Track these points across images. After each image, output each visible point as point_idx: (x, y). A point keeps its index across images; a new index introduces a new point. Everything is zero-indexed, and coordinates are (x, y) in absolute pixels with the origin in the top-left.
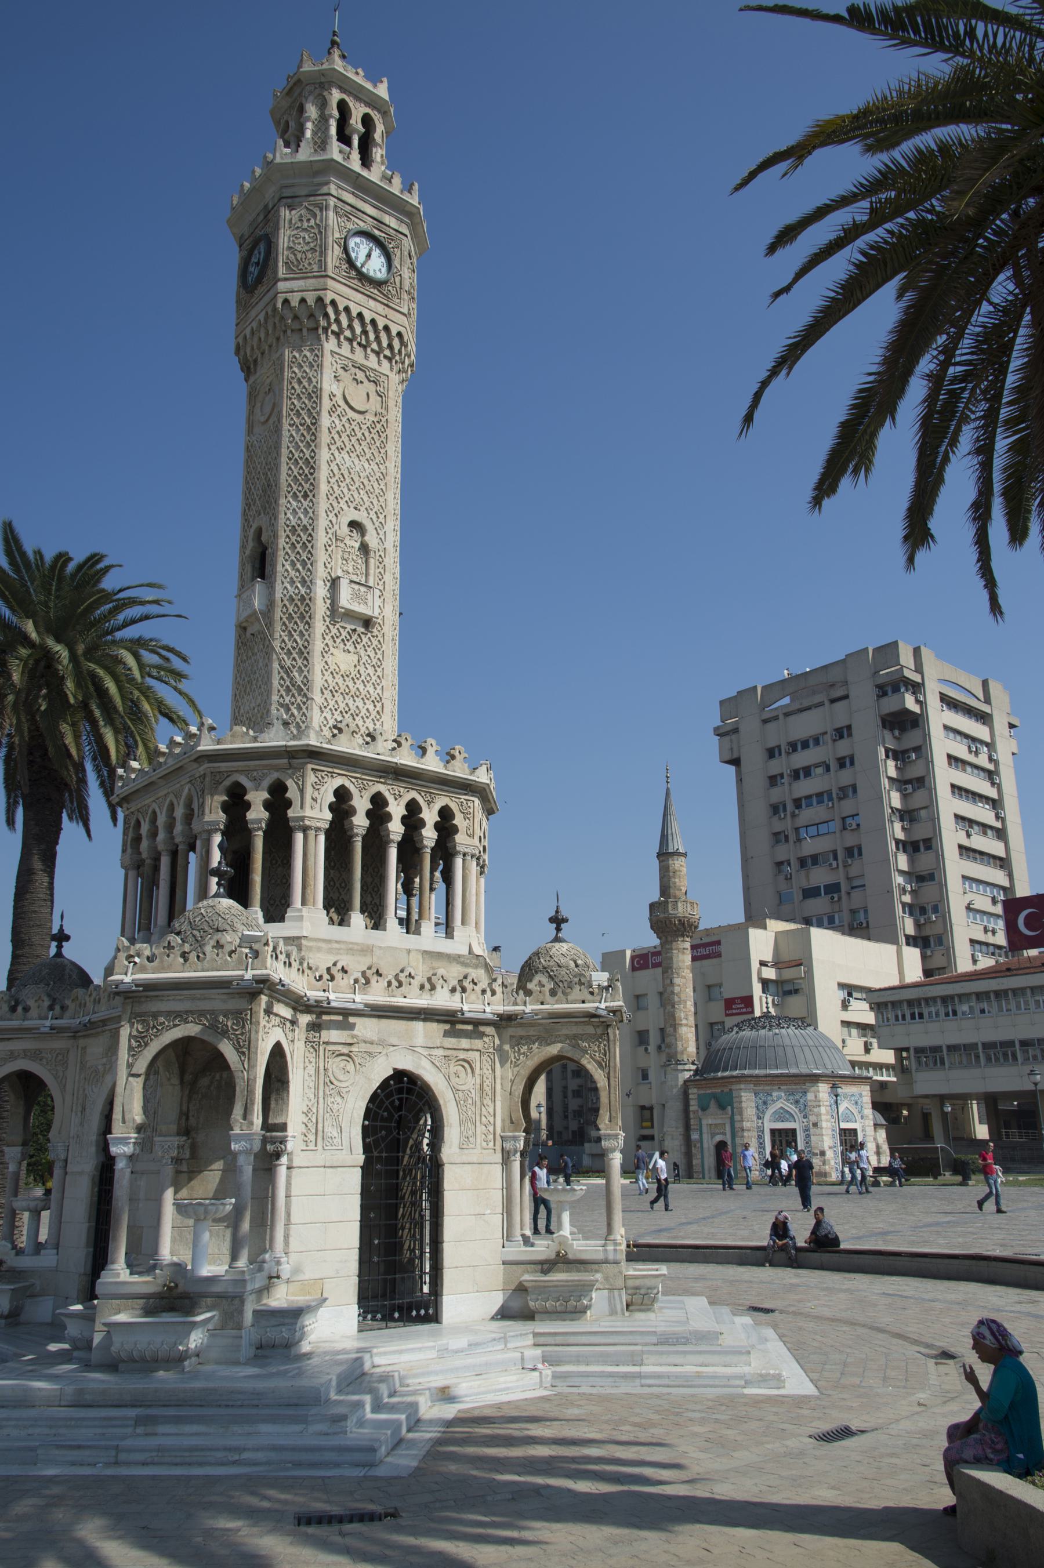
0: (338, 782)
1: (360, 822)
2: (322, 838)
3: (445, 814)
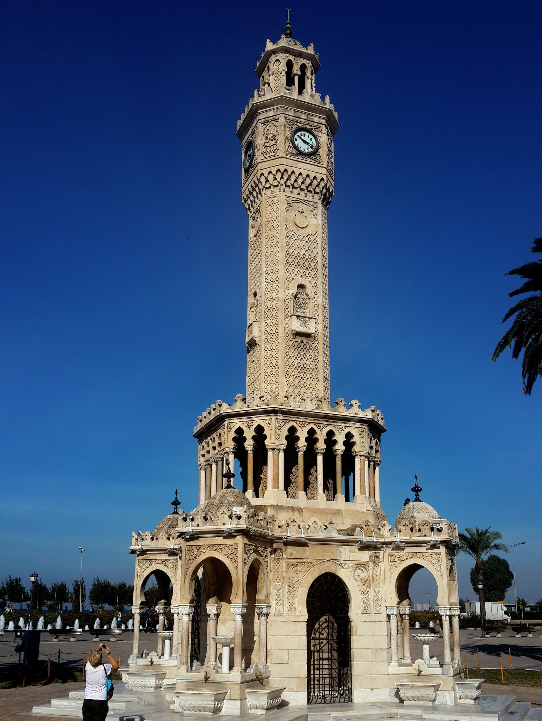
0: (289, 425)
1: (302, 444)
2: (282, 455)
3: (349, 436)
